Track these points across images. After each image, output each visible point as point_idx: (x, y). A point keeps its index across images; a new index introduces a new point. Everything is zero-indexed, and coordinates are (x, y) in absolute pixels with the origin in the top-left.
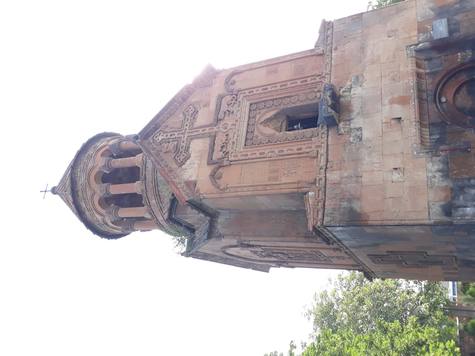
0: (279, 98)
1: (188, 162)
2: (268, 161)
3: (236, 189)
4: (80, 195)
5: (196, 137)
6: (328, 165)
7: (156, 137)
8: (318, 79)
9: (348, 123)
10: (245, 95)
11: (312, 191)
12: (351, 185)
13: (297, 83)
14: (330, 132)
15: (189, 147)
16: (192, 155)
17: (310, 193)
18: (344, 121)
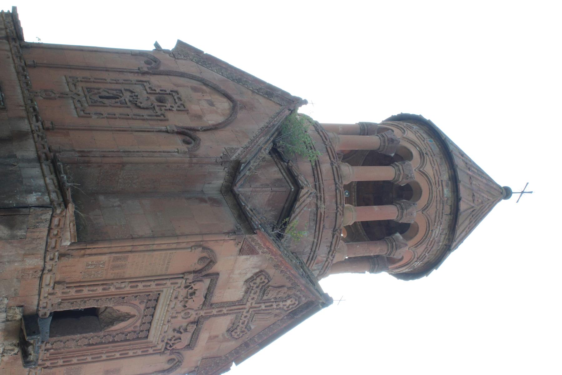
0: (105, 343)
1: (249, 275)
2: (126, 279)
3: (178, 247)
4: (449, 207)
5: (233, 304)
6: (41, 273)
7: (295, 303)
8: (48, 364)
9: (9, 318)
10: (154, 348)
11: (65, 246)
12: (10, 254)
13: (78, 360)
14: (35, 308)
15: (246, 292)
16: (242, 283)
17: (69, 244)
18: (15, 320)
